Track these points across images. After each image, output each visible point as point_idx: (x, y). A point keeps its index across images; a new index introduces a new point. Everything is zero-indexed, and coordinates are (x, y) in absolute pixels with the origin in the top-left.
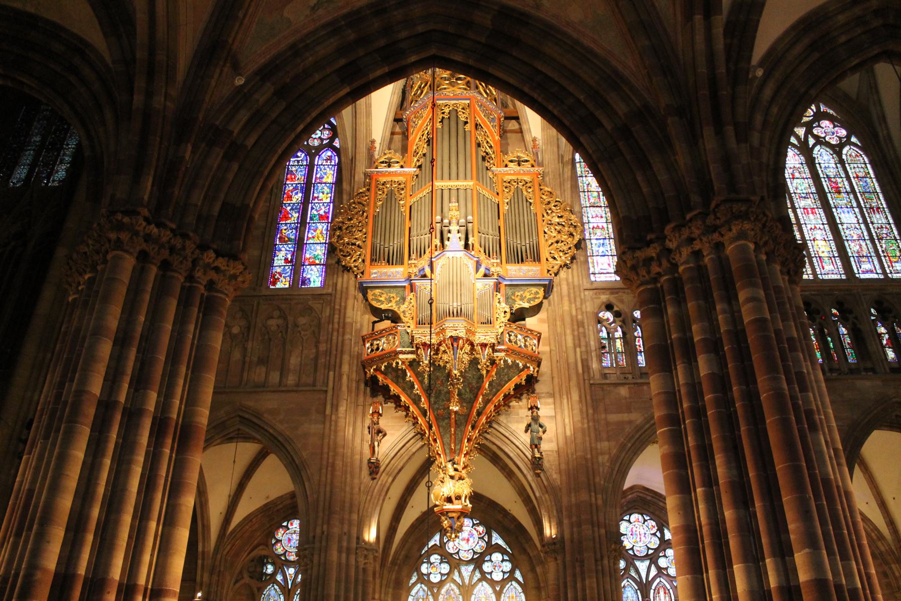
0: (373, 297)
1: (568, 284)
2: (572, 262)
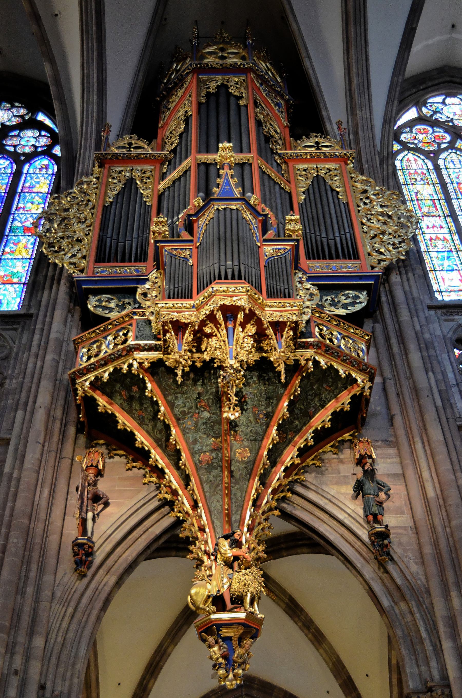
0: (97, 303)
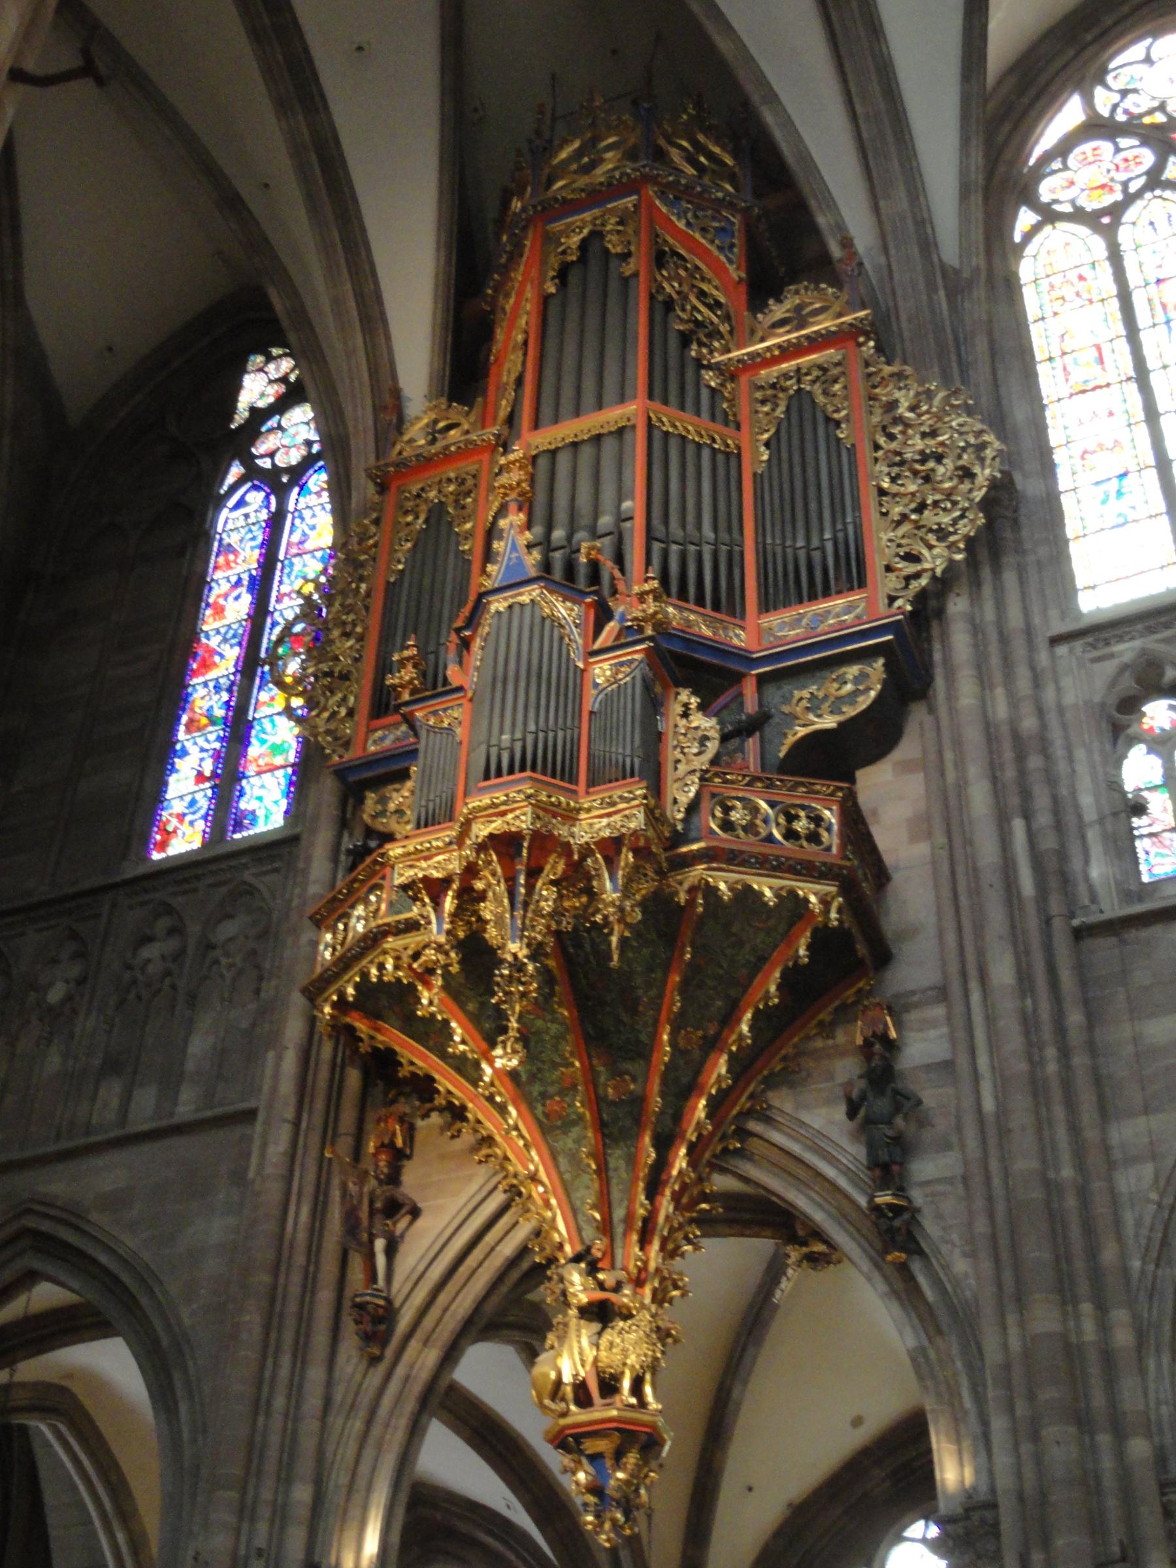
1: (976, 629)
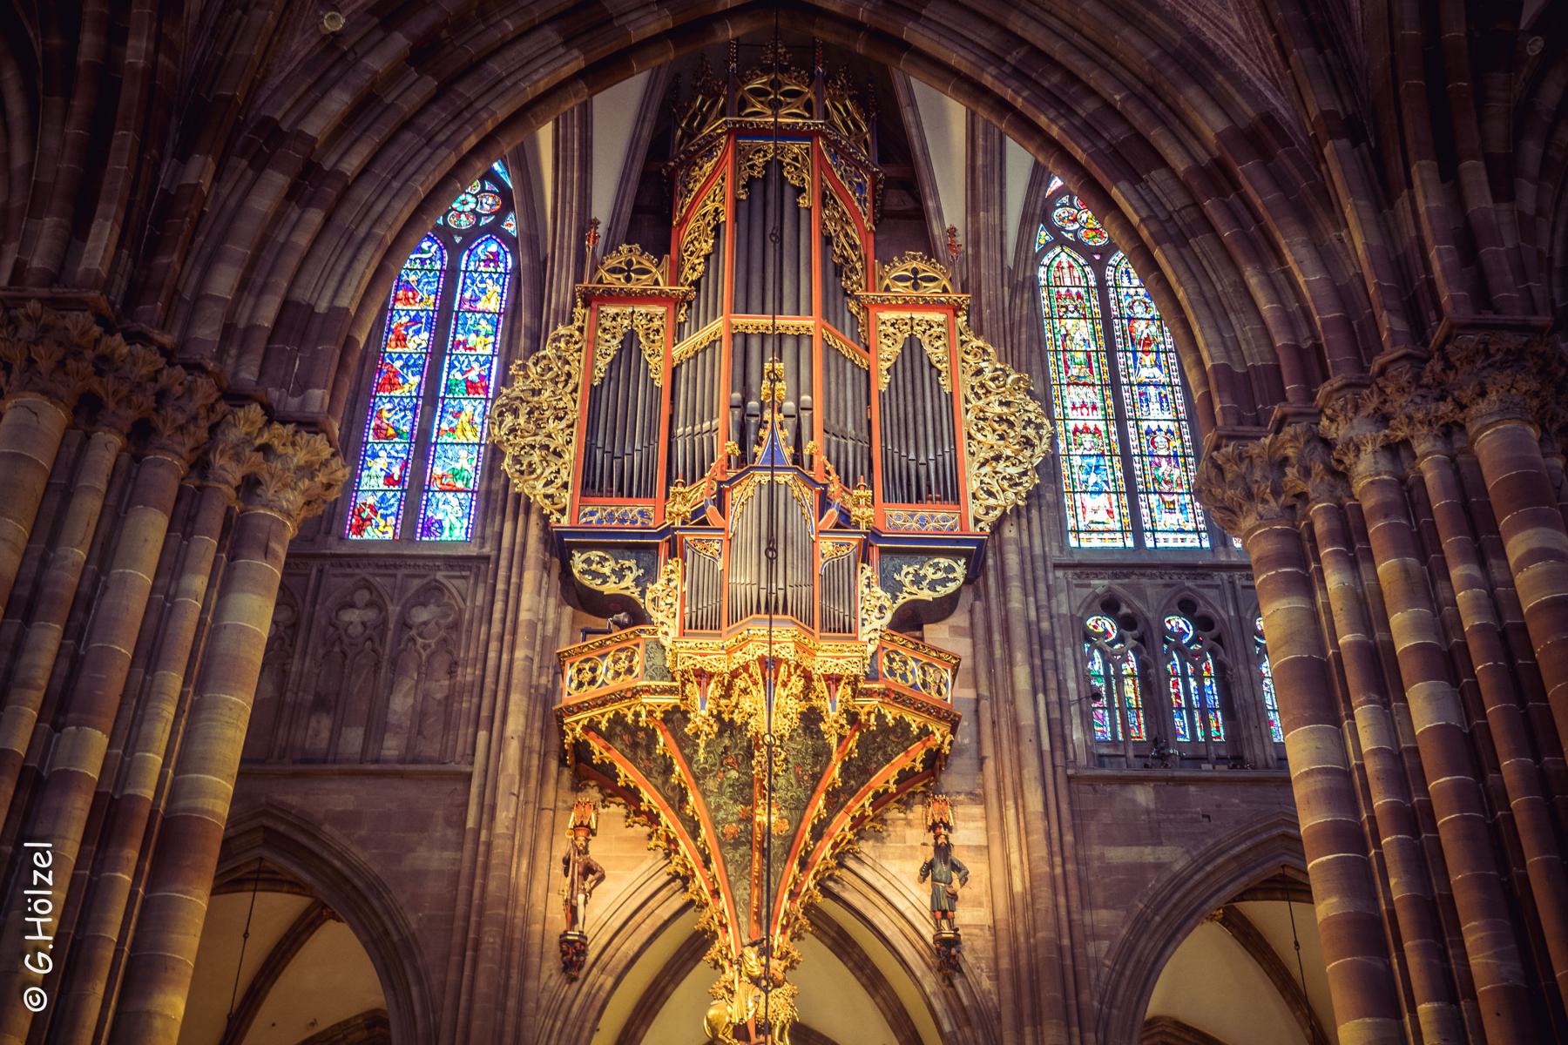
0: (586, 566)
1: (1021, 552)
2: (1028, 507)
